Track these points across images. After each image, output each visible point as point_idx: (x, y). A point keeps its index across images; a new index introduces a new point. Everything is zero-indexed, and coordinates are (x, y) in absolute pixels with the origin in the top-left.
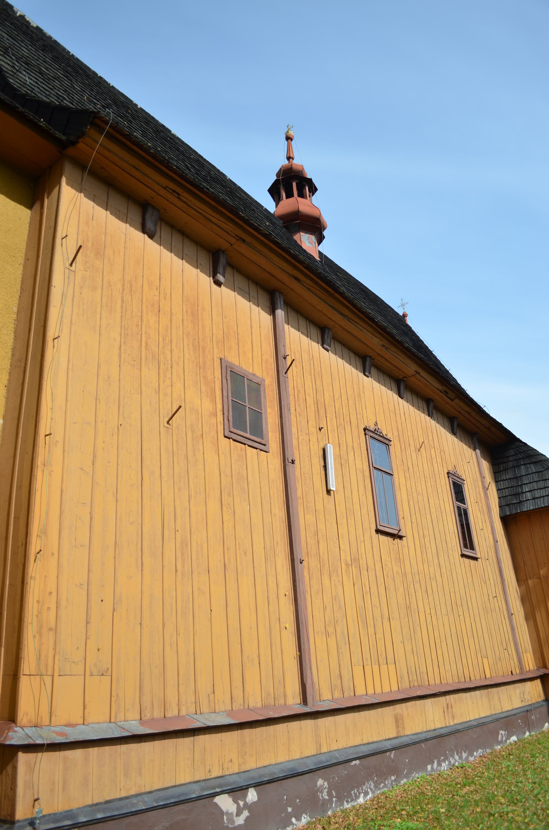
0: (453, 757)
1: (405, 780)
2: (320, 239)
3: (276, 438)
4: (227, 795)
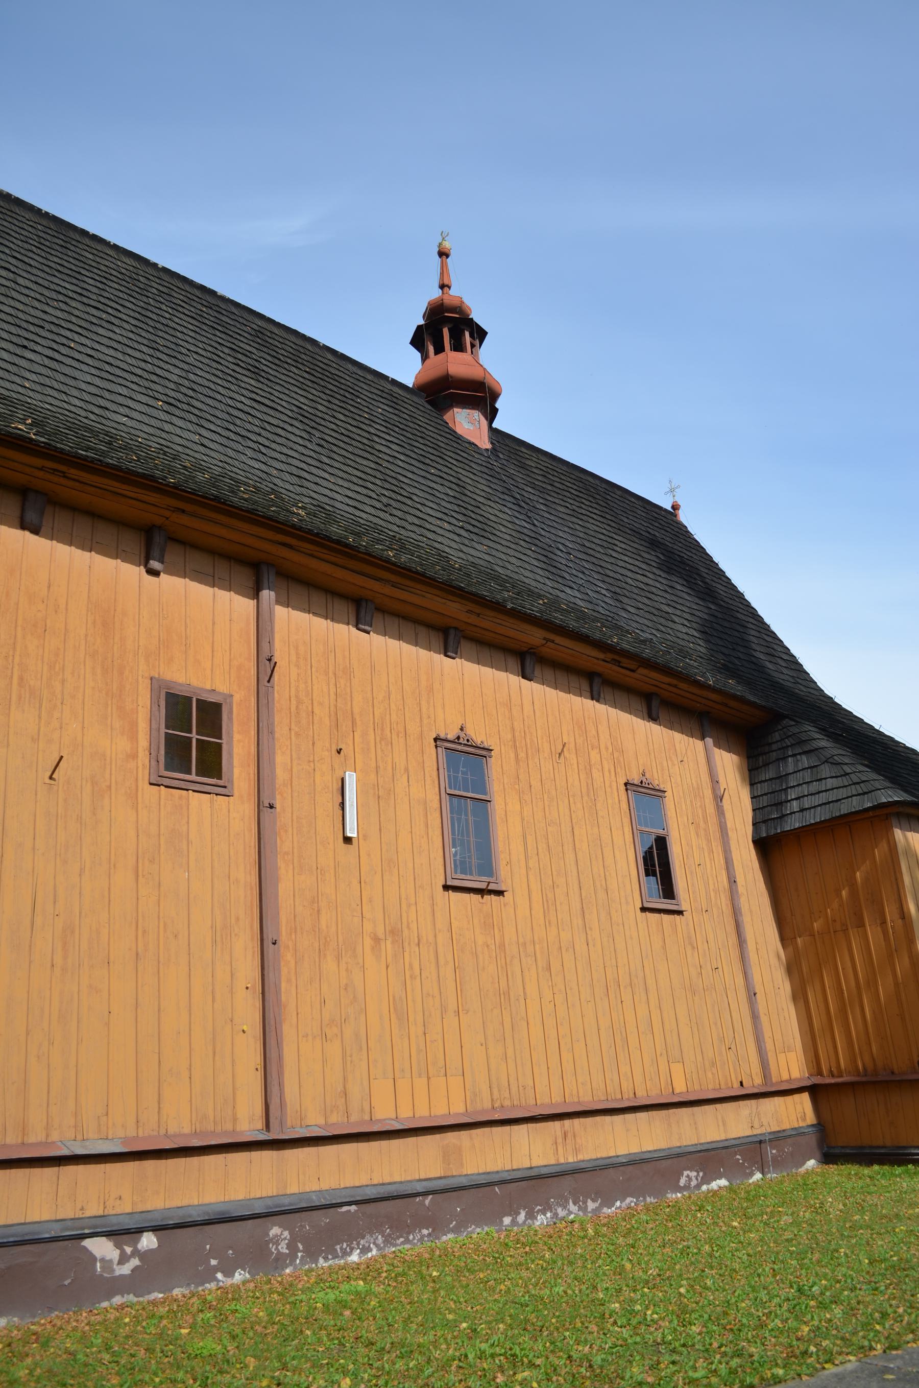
0: (565, 1207)
1: (450, 1236)
2: (491, 414)
3: (249, 774)
4: (104, 1238)
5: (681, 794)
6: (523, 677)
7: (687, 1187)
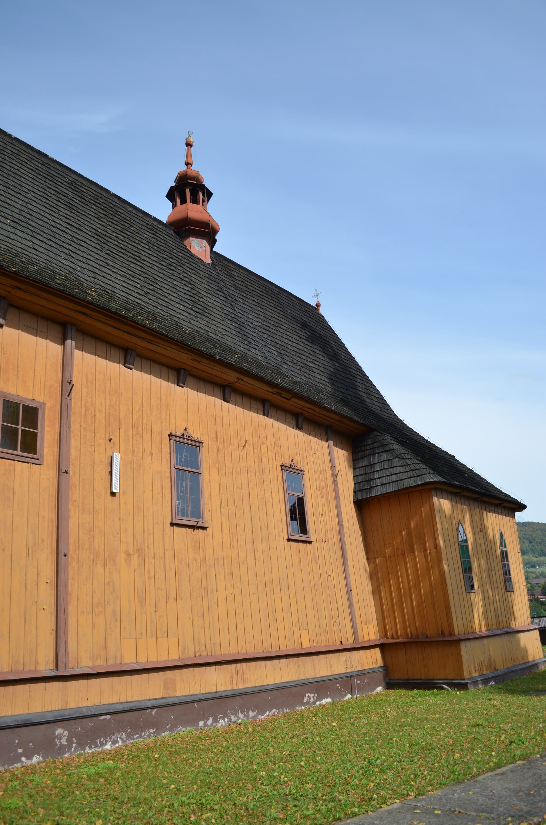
0: (236, 715)
1: (167, 733)
2: (213, 242)
5: (314, 473)
6: (223, 400)
7: (308, 703)
